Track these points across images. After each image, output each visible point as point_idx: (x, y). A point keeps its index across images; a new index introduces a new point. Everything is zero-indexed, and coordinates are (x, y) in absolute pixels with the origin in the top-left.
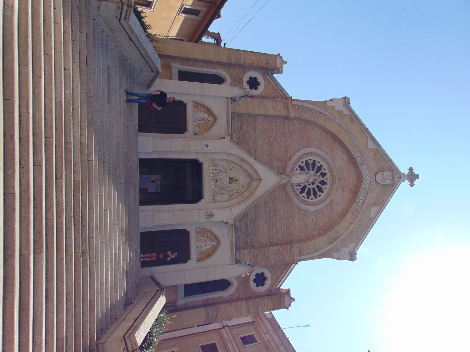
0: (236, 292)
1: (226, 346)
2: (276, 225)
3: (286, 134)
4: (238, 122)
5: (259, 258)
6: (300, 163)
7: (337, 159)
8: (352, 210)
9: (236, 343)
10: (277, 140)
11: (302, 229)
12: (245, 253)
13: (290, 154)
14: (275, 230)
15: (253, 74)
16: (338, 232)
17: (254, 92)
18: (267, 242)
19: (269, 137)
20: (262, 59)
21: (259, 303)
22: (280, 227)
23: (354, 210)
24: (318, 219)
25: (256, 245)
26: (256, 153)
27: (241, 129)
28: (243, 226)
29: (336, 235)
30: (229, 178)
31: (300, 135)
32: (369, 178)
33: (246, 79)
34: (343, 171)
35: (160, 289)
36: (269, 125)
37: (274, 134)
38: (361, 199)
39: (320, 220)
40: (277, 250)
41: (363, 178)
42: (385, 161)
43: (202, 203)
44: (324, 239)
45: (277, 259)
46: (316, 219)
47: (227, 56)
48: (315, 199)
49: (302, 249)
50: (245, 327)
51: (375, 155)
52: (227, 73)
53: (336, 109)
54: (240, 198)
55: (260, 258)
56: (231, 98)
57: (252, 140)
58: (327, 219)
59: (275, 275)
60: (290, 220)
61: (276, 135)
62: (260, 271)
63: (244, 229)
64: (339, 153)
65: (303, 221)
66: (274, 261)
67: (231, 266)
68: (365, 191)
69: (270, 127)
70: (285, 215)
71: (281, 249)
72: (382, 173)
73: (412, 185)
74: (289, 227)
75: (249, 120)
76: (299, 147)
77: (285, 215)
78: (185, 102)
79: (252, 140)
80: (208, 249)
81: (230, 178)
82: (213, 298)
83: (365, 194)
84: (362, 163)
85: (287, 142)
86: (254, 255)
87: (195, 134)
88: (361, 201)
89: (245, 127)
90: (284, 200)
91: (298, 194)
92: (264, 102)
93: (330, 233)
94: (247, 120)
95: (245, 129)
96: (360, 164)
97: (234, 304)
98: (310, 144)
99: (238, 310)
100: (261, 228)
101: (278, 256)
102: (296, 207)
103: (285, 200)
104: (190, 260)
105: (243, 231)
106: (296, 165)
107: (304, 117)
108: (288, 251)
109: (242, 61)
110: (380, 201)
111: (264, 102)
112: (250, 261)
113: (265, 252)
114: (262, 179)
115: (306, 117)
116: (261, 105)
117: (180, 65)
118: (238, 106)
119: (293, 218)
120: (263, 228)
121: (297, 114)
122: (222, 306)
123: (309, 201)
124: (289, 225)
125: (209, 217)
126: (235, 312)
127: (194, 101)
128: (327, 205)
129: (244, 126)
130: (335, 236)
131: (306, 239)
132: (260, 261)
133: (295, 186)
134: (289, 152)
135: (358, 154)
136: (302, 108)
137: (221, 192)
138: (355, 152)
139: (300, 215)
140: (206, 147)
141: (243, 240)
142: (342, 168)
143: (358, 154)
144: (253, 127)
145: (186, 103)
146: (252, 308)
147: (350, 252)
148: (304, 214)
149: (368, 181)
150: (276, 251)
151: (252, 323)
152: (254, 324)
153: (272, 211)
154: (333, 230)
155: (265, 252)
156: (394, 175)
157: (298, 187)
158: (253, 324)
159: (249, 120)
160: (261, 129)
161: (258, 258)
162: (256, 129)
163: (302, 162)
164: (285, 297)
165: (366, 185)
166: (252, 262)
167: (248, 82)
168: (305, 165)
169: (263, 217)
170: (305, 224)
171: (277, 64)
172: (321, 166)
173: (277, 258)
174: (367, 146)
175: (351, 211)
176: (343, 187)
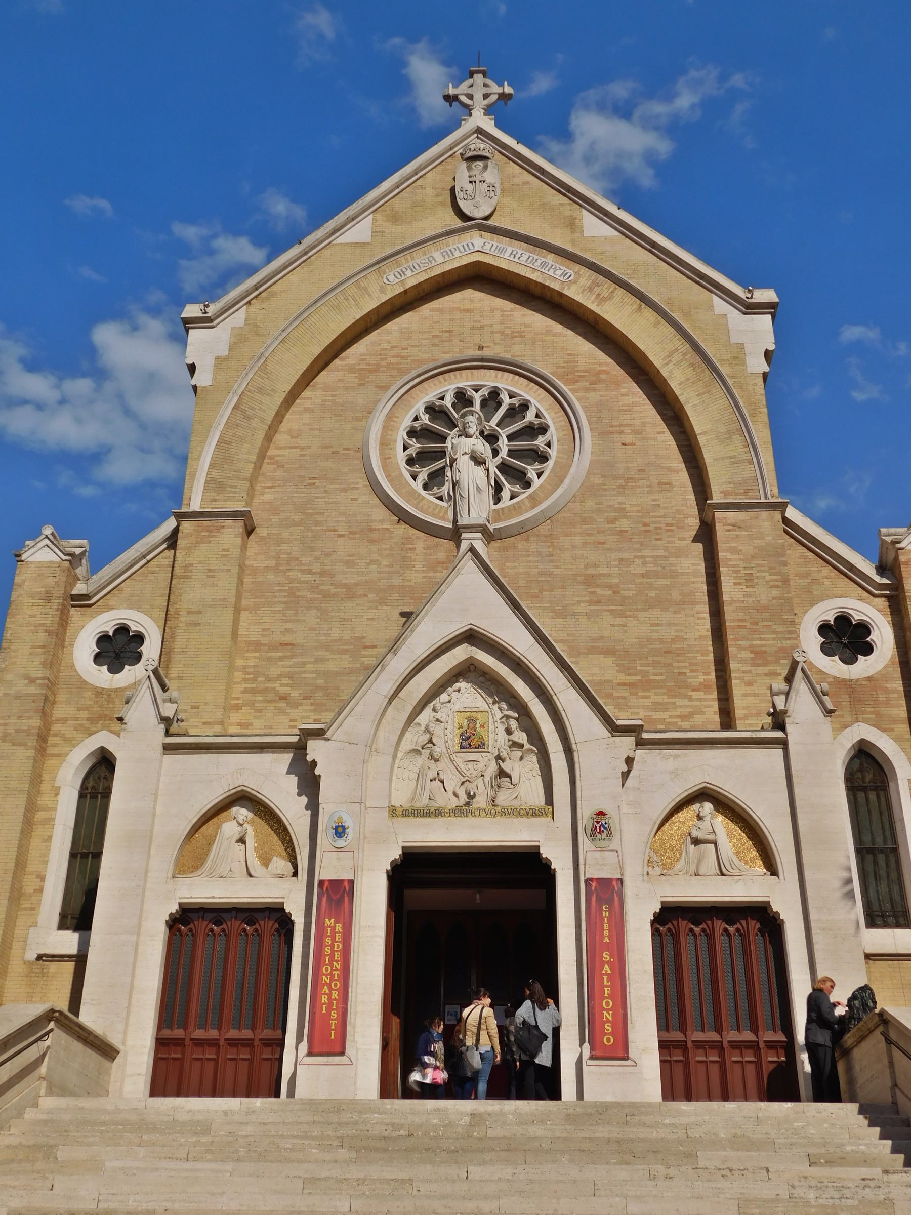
0: (892, 730)
3: (310, 534)
4: (260, 711)
5: (763, 642)
6: (418, 486)
7: (404, 353)
8: (593, 303)
10: (330, 567)
11: (660, 484)
12: (745, 695)
14: (662, 582)
16: (670, 355)
17: (151, 650)
20: (31, 616)
22: (650, 563)
24: (624, 426)
26: (374, 647)
27: (283, 698)
28: (643, 697)
29: (681, 361)
30: (462, 747)
31: (314, 484)
33: (101, 676)
35: (881, 1028)
40: (735, 575)
41: (477, 263)
44: (695, 406)
45: (768, 577)
46: (622, 432)
47: (14, 744)
48: (548, 434)
49: (730, 483)
51: (395, 219)
53: (226, 353)
55: (763, 639)
56: (167, 733)
57: (328, 660)
59: (827, 583)
60: (624, 524)
61: (310, 572)
63: (656, 694)
64: (385, 345)
65: (628, 479)
66: (777, 586)
67: (792, 748)
68: (525, 258)
69: (281, 591)
70: (604, 543)
71: (730, 560)
74: (649, 531)
75: (254, 667)
76: (357, 489)
77: (604, 543)
78: (174, 908)
79: (328, 660)
80: (730, 835)
81: (464, 744)
83: (536, 257)
85: (335, 530)
86: (752, 659)
88: (562, 272)
89: (276, 685)
90: (549, 547)
91: (530, 497)
92: (189, 613)
94: (251, 676)
95: (287, 685)
98: (348, 449)
100: (652, 631)
101: (758, 571)
102: (575, 502)
103: (549, 544)
104: (768, 902)
105: (665, 698)
106: (424, 502)
107: (251, 466)
108: (737, 536)
109: (33, 689)
110: (561, 204)
111: (189, 613)
112: (775, 674)
114: (470, 626)
115: (250, 462)
116: (199, 625)
118: (197, 707)
119: (617, 514)
120: (652, 625)
121: (235, 492)
123: (557, 457)
124: (644, 528)
125: (605, 828)
127: (170, 875)
129: (274, 688)
130: (685, 364)
132: (774, 639)
133: (500, 505)
134: (375, 525)
135: (391, 278)
136: (215, 473)
138: (382, 290)
139: (606, 490)
140: (344, 832)
142: (437, 336)
144: (280, 654)
145: (176, 907)
148: (603, 476)
149: (488, 246)
150: (740, 578)
153: (590, 590)
154: (664, 373)
156: (467, 155)
157: (506, 494)
159: (251, 670)
160: (287, 627)
161: (765, 646)
162: (286, 644)
163: (414, 478)
165: (503, 250)
166: (779, 669)
167: (115, 669)
168: (423, 466)
169: (612, 625)
170: (640, 470)
171: (51, 562)
173: (764, 577)
175: (593, 307)
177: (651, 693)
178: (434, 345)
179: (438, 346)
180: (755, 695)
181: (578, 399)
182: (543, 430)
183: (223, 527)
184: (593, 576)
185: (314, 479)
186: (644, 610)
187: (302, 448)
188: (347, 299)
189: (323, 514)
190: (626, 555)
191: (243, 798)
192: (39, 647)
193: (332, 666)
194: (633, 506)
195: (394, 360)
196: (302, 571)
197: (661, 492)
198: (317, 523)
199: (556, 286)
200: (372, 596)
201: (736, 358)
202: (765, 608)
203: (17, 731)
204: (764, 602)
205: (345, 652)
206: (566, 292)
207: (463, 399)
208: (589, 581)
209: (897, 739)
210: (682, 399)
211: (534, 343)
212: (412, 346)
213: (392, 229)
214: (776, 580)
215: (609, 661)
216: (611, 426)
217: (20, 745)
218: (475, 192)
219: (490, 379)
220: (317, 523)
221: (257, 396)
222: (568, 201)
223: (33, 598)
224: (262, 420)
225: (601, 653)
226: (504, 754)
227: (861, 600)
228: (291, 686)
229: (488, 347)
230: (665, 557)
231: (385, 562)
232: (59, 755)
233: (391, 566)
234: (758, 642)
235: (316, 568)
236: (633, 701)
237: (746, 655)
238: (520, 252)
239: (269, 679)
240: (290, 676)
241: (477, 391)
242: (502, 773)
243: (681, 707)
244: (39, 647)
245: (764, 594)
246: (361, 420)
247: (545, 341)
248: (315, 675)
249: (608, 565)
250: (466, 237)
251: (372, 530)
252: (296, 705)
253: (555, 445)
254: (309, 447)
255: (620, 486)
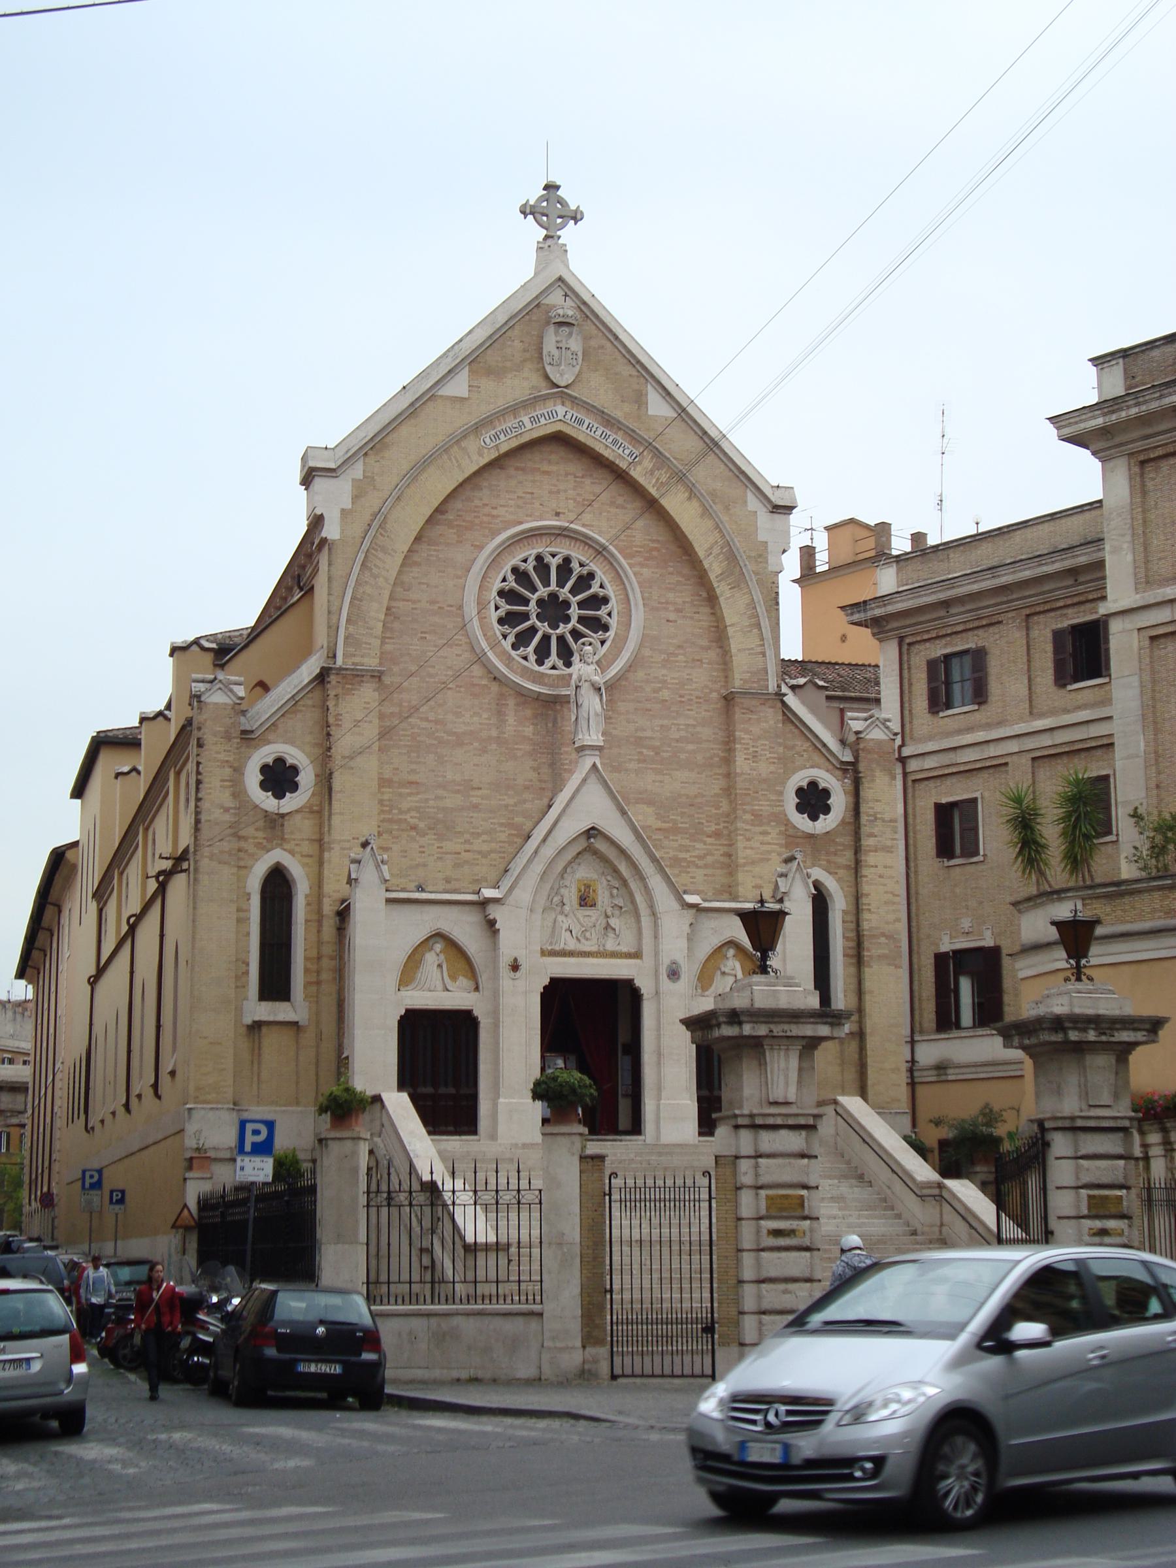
0: (836, 873)
1: (967, 768)
2: (677, 741)
4: (397, 838)
6: (507, 644)
7: (495, 512)
8: (653, 486)
9: (960, 732)
11: (694, 660)
13: (481, 678)
14: (691, 747)
15: (253, 779)
16: (711, 548)
18: (719, 774)
19: (436, 742)
21: (871, 815)
22: (682, 730)
23: (654, 480)
25: (725, 806)
26: (480, 789)
27: (414, 828)
28: (673, 840)
29: (718, 555)
32: (561, 410)
33: (267, 801)
34: (532, 493)
36: (401, 740)
37: (424, 724)
38: (621, 449)
39: (671, 596)
41: (560, 432)
42: (509, 333)
43: (644, 984)
44: (727, 599)
45: (768, 755)
46: (666, 609)
47: (220, 863)
50: (914, 681)
51: (490, 372)
52: (257, 860)
53: (350, 507)
54: (634, 885)
55: (762, 805)
58: (671, 569)
60: (665, 694)
61: (427, 720)
62: (792, 800)
63: (682, 838)
66: (774, 763)
68: (599, 433)
72: (546, 359)
73: (576, 217)
75: (389, 800)
76: (461, 645)
82: (844, 937)
84: (513, 430)
87: (477, 989)
89: (407, 817)
93: (712, 576)
96: (516, 436)
97: (866, 888)
98: (451, 606)
99: (881, 876)
105: (687, 842)
108: (750, 719)
113: (749, 789)
115: (379, 621)
117: (246, 999)
122: (867, 920)
126: (885, 885)
128: (631, 566)
129: (406, 820)
131: (721, 647)
134: (476, 681)
135: (488, 440)
137: (617, 932)
141: (710, 844)
143: (488, 440)
146: (881, 836)
147: (772, 512)
149: (569, 416)
151: (905, 647)
152: (908, 640)
154: (706, 564)
155: (749, 789)
158: (910, 644)
159: (388, 803)
161: (761, 810)
164: (867, 737)
165: (581, 422)
166: (769, 829)
167: (279, 795)
170: (679, 647)
171: (226, 704)
172: (515, 570)
174: (462, 400)
176: (579, 499)
177: (678, 838)
178: (519, 507)
179: (522, 507)
180: (752, 848)
181: (635, 574)
182: (605, 600)
183: (362, 681)
184: (641, 738)
185: (425, 633)
186: (677, 770)
187: (414, 602)
188: (450, 459)
189: (434, 667)
190: (665, 722)
191: (439, 935)
192: (226, 781)
193: (448, 803)
194: (674, 678)
195: (485, 519)
196: (421, 719)
197: (692, 668)
198: (431, 676)
199: (623, 465)
200: (476, 744)
201: (760, 556)
202: (765, 781)
203: (222, 852)
204: (764, 775)
205: (458, 792)
206: (632, 473)
207: (541, 565)
208: (639, 742)
209: (839, 880)
210: (718, 591)
211: (601, 514)
212: (501, 506)
213: (487, 384)
214: (775, 758)
215: (650, 810)
216: (659, 603)
217: (225, 863)
218: (560, 358)
219: (564, 549)
220: (431, 676)
221: (381, 555)
222: (637, 374)
223: (215, 736)
224: (386, 580)
225: (645, 803)
226: (609, 913)
227: (827, 771)
228: (420, 819)
229: (564, 513)
230: (694, 726)
231: (485, 715)
232: (245, 867)
233: (489, 719)
234: (756, 808)
235: (432, 716)
236: (666, 843)
237: (748, 817)
238: (596, 425)
239: (401, 812)
240: (417, 809)
241: (554, 556)
242: (608, 927)
243: (698, 849)
244: (226, 781)
245: (765, 768)
246: (460, 577)
247: (609, 512)
248: (436, 810)
249: (653, 730)
250: (550, 403)
251: (474, 685)
252: (424, 835)
253: (615, 614)
254: (419, 601)
255: (664, 660)
